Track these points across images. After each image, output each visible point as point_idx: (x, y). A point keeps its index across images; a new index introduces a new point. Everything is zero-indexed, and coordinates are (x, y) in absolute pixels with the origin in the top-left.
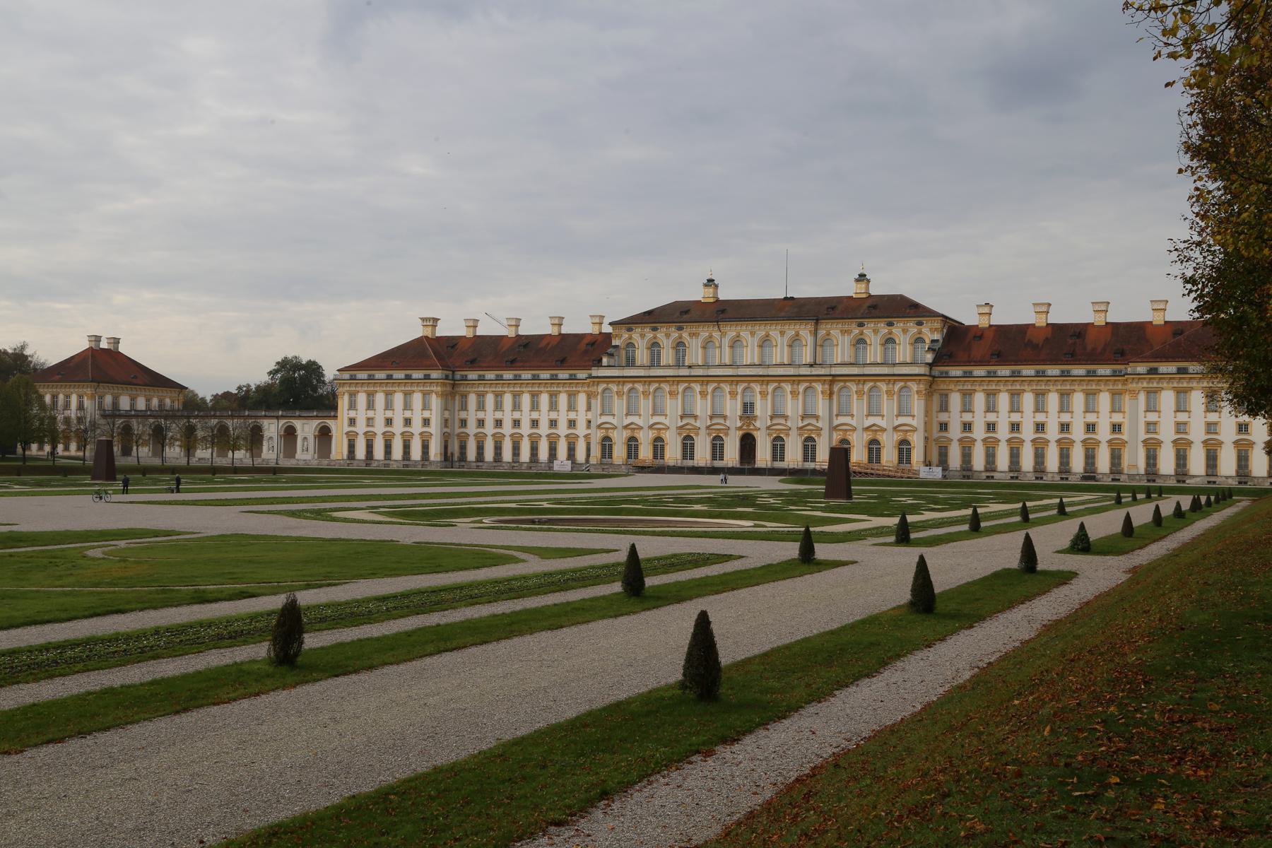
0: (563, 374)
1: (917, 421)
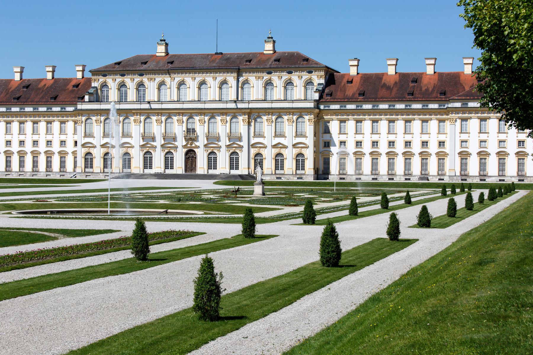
1: (310, 141)
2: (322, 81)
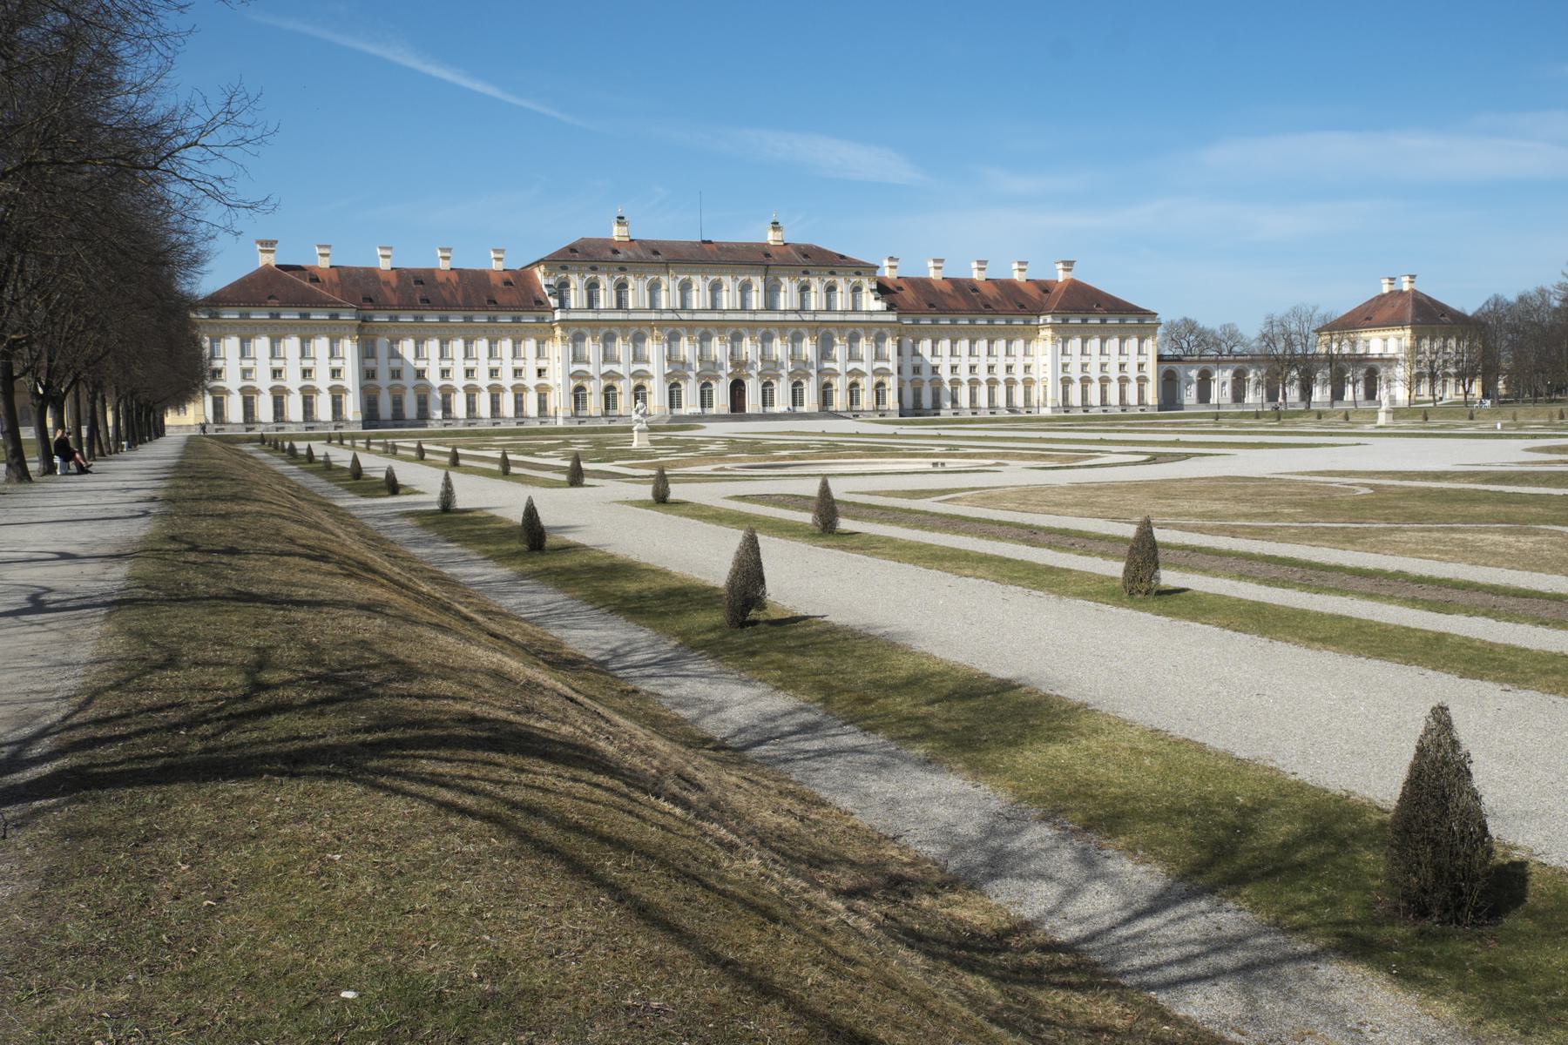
0: (505, 319)
1: (892, 366)
2: (874, 286)
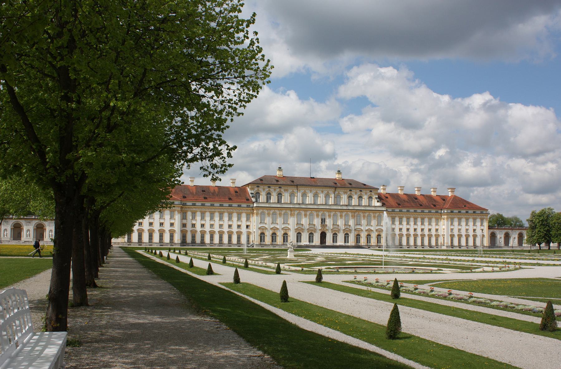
2: (377, 197)
